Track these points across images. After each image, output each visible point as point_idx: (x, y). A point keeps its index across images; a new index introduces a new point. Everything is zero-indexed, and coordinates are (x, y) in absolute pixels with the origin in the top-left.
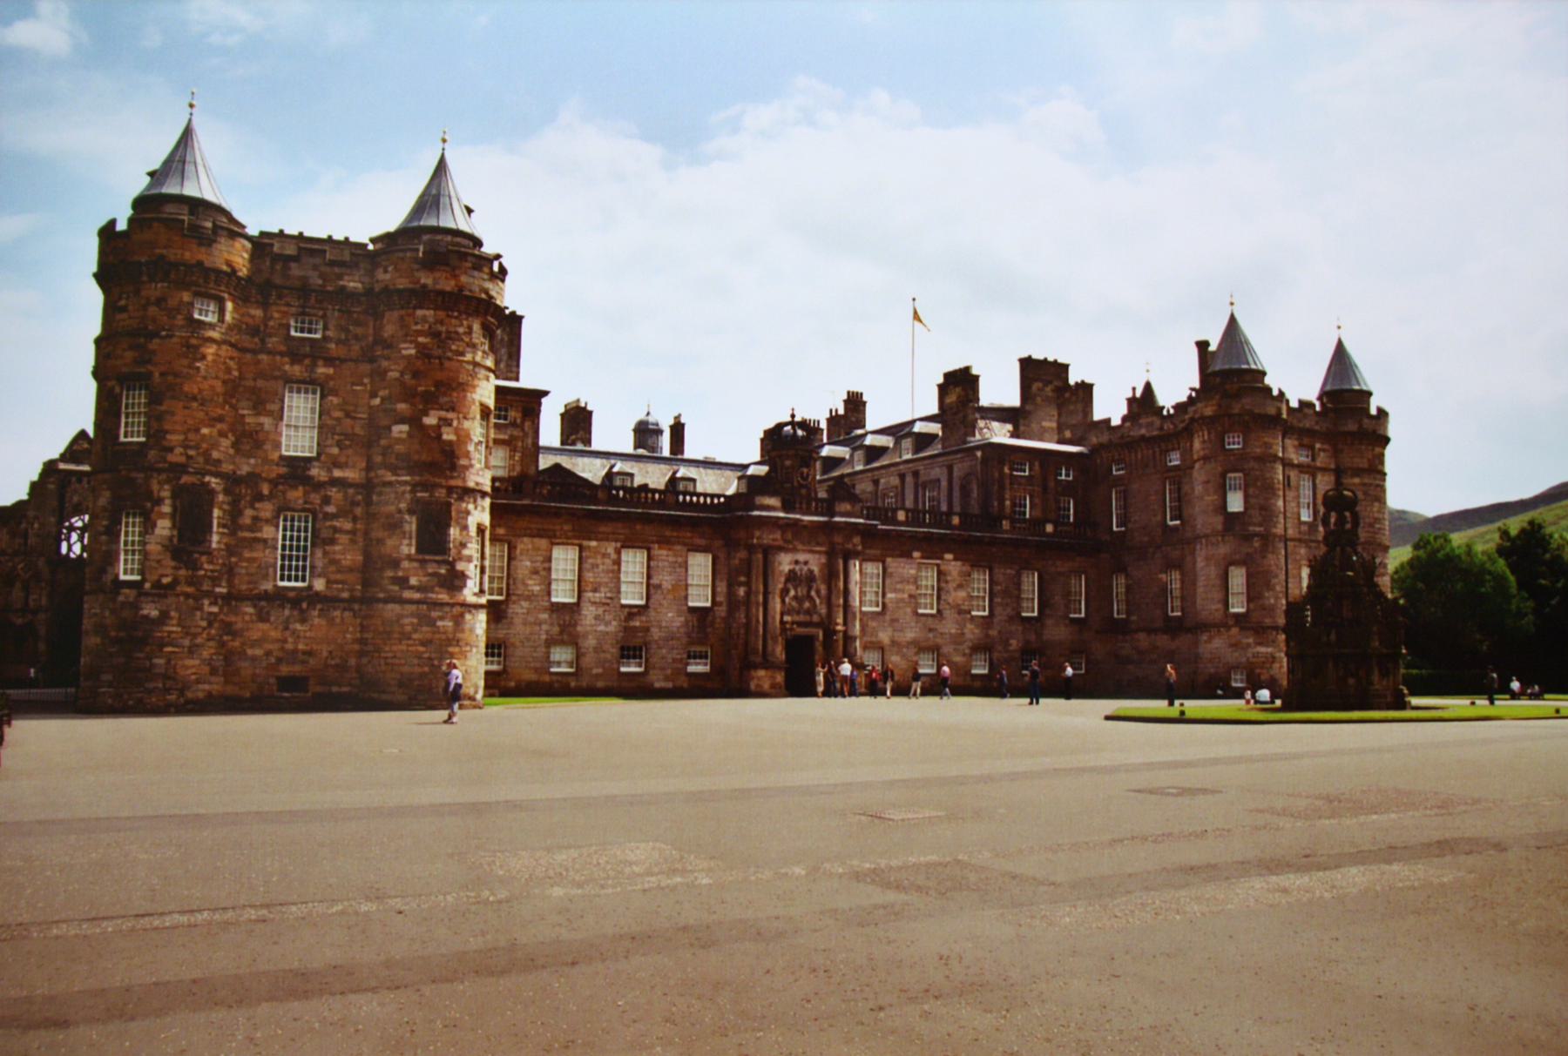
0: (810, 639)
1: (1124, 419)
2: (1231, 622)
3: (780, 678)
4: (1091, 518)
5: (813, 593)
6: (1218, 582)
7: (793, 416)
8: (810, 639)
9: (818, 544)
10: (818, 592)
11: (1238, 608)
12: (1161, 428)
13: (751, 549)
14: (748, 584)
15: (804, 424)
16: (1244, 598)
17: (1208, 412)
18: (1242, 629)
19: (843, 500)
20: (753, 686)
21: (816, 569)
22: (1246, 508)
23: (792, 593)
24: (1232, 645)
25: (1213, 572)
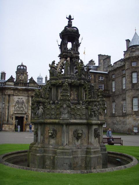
0: (23, 118)
1: (115, 63)
2: (133, 114)
3: (13, 127)
4: (108, 89)
5: (23, 106)
6: (130, 102)
7: (22, 64)
8: (23, 118)
9: (25, 94)
10: (25, 106)
11: (135, 109)
12: (121, 64)
13: (5, 95)
14: (4, 104)
15: (23, 66)
16: (137, 106)
17: (127, 57)
18: (137, 115)
19: (32, 83)
20: (3, 129)
21: (25, 101)
22: (137, 82)
23: (17, 106)
24: (134, 120)
25: (128, 100)
